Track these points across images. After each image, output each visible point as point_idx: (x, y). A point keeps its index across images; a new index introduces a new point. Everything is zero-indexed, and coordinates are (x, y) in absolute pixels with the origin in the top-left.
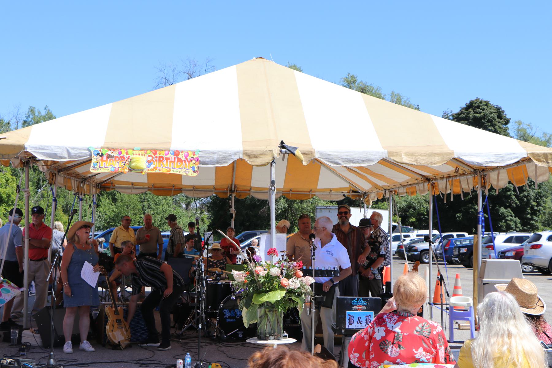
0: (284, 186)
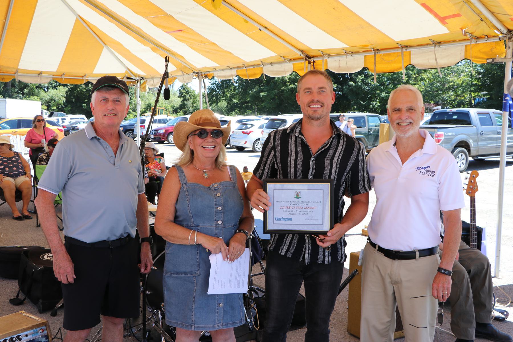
0: (58, 69)
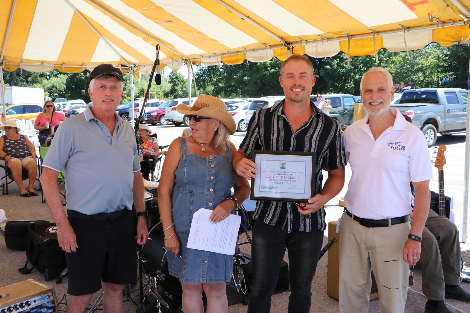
0: (58, 59)
